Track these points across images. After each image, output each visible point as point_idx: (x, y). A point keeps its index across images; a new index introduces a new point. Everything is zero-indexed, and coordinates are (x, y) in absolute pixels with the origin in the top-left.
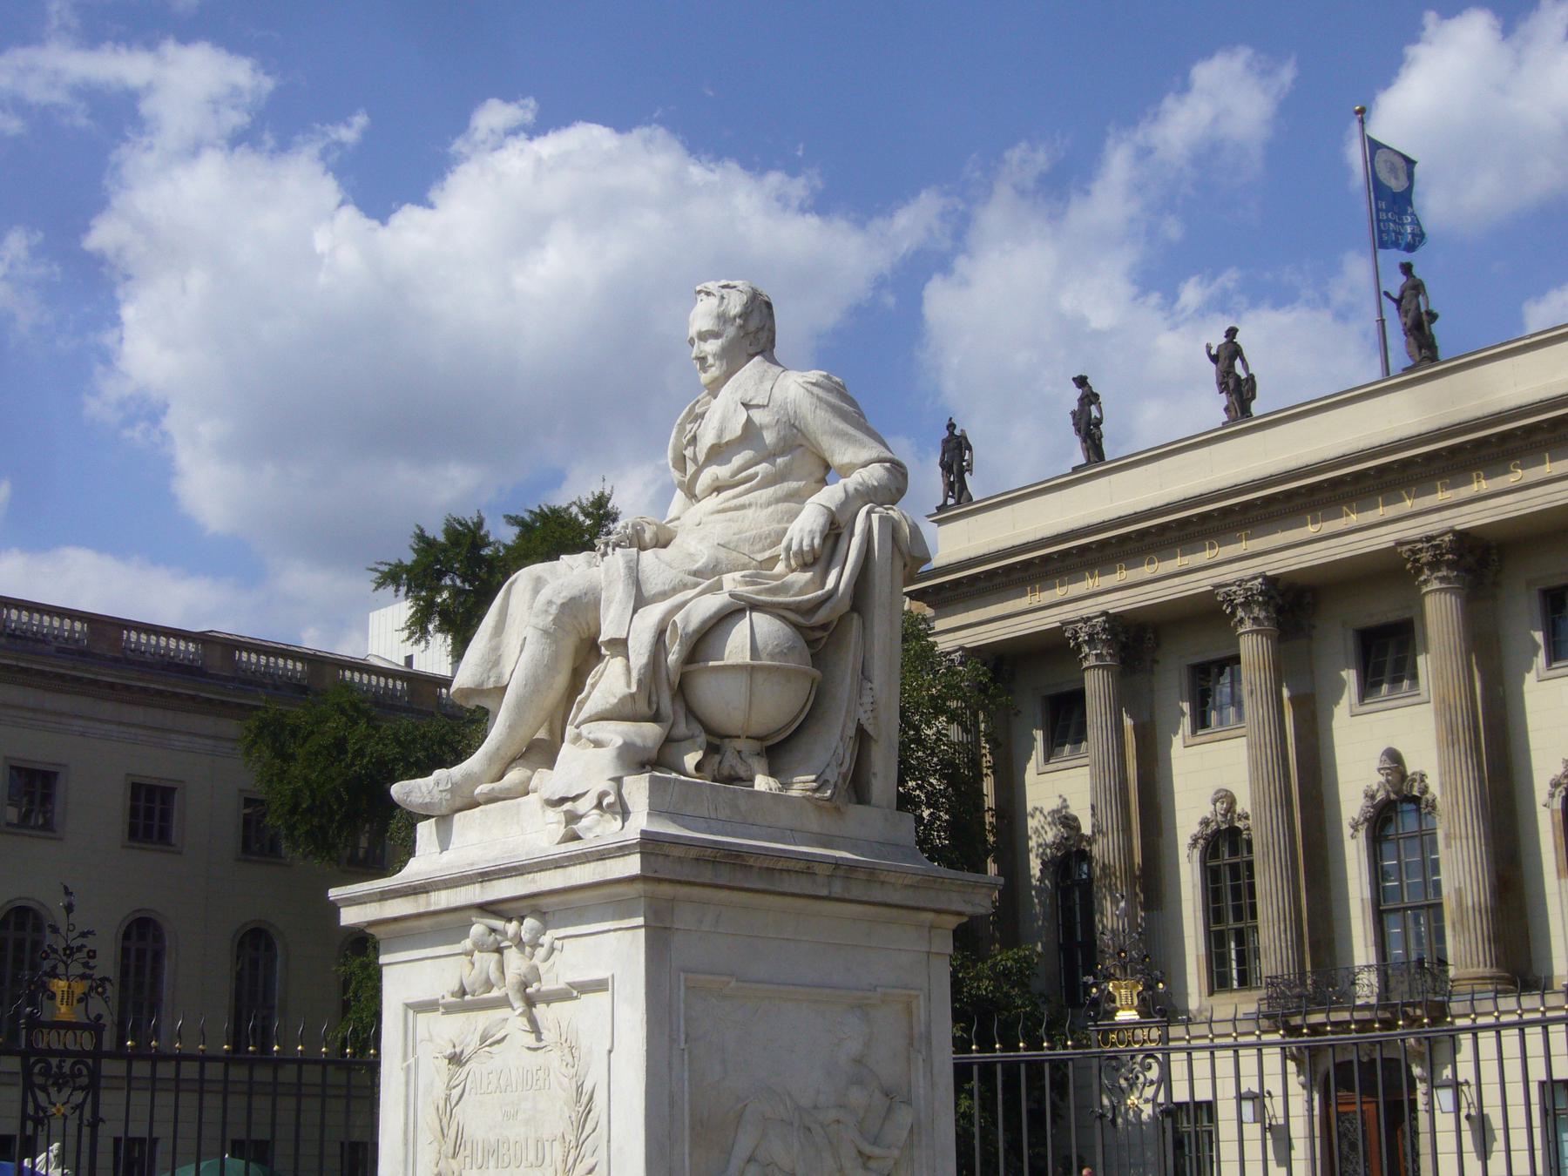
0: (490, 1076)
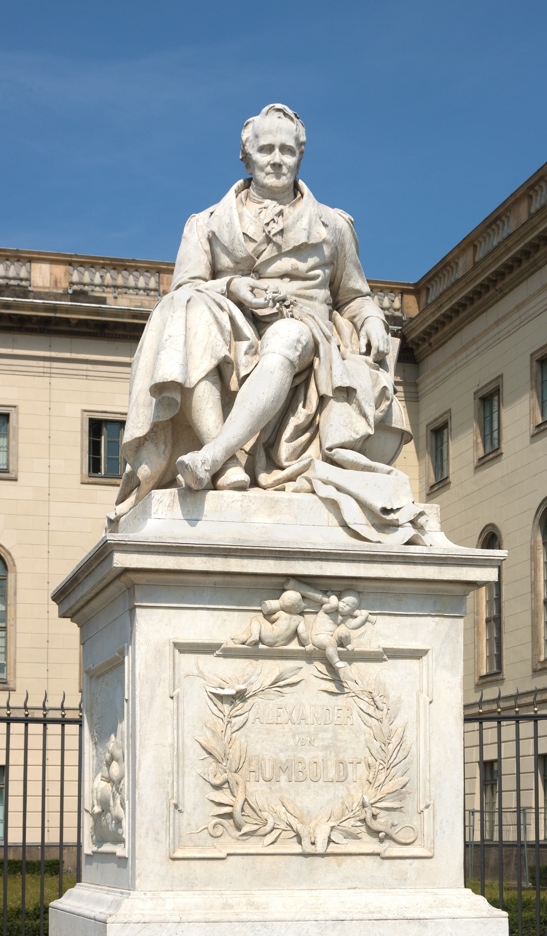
0: (280, 710)
